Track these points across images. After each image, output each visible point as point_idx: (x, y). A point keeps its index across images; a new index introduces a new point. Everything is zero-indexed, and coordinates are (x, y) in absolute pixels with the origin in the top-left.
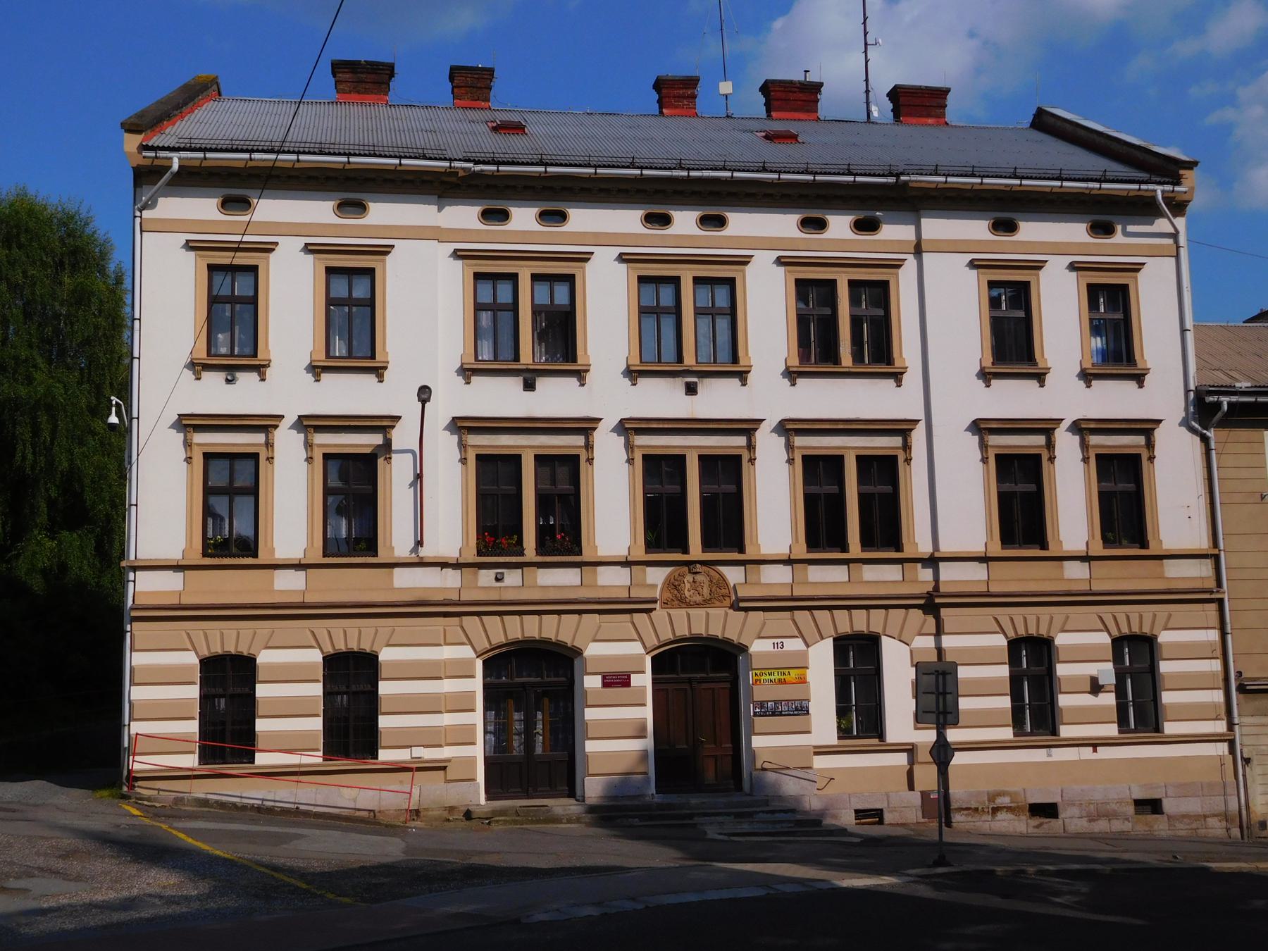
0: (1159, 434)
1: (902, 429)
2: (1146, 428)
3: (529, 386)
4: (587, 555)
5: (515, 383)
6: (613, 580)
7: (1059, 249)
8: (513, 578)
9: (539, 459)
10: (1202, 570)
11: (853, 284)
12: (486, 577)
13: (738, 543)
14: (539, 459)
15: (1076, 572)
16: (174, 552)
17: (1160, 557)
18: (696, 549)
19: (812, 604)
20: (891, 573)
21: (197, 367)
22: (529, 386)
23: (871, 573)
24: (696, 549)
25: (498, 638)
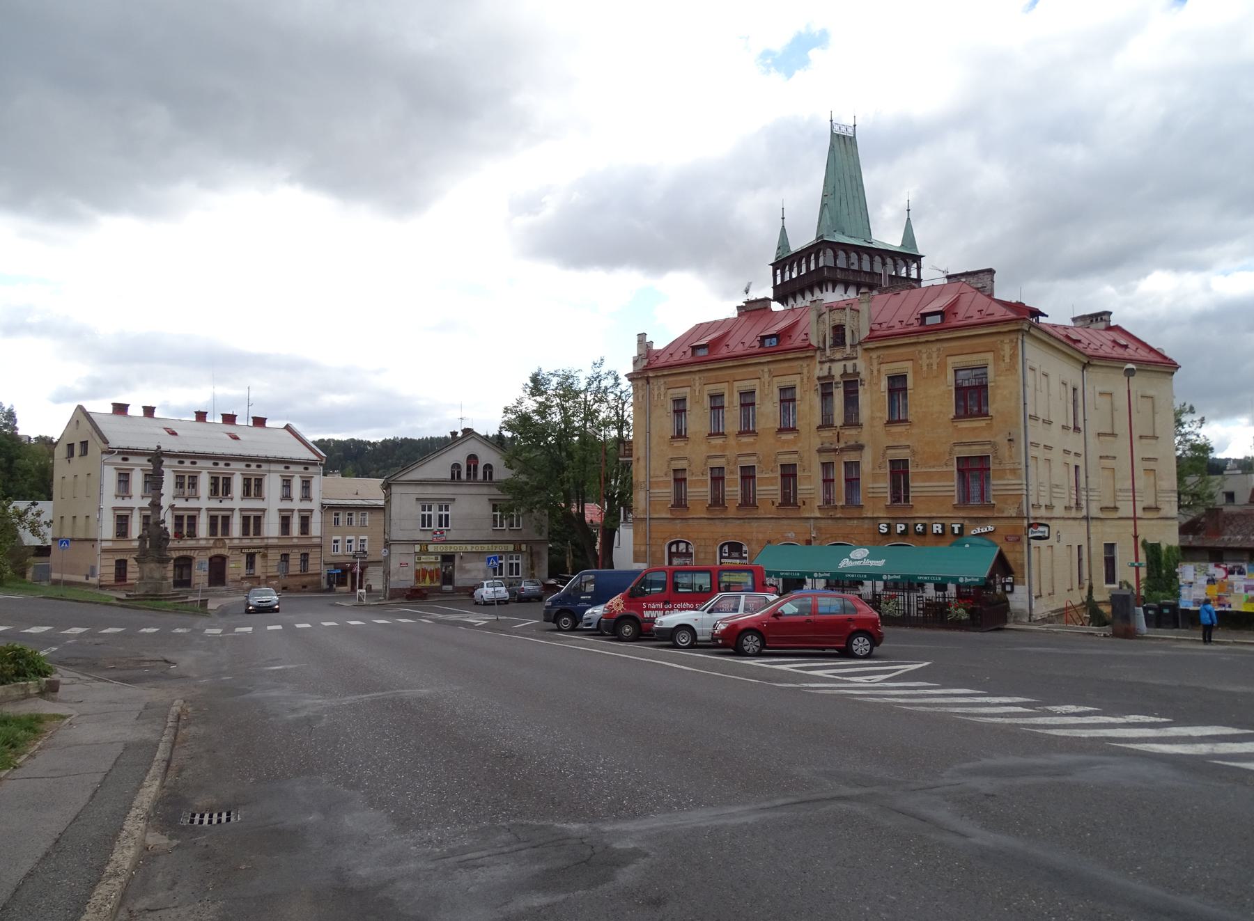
0: (314, 512)
1: (264, 510)
2: (311, 511)
3: (187, 500)
4: (197, 538)
5: (184, 500)
6: (203, 543)
7: (297, 473)
8: (181, 542)
9: (188, 517)
10: (319, 540)
11: (255, 479)
12: (176, 543)
13: (228, 535)
14: (188, 517)
15: (295, 541)
16: (110, 537)
17: (311, 538)
18: (219, 536)
19: (242, 548)
20: (258, 541)
21: (117, 496)
22: (187, 500)
23: (255, 541)
24: (219, 536)
25: (178, 555)
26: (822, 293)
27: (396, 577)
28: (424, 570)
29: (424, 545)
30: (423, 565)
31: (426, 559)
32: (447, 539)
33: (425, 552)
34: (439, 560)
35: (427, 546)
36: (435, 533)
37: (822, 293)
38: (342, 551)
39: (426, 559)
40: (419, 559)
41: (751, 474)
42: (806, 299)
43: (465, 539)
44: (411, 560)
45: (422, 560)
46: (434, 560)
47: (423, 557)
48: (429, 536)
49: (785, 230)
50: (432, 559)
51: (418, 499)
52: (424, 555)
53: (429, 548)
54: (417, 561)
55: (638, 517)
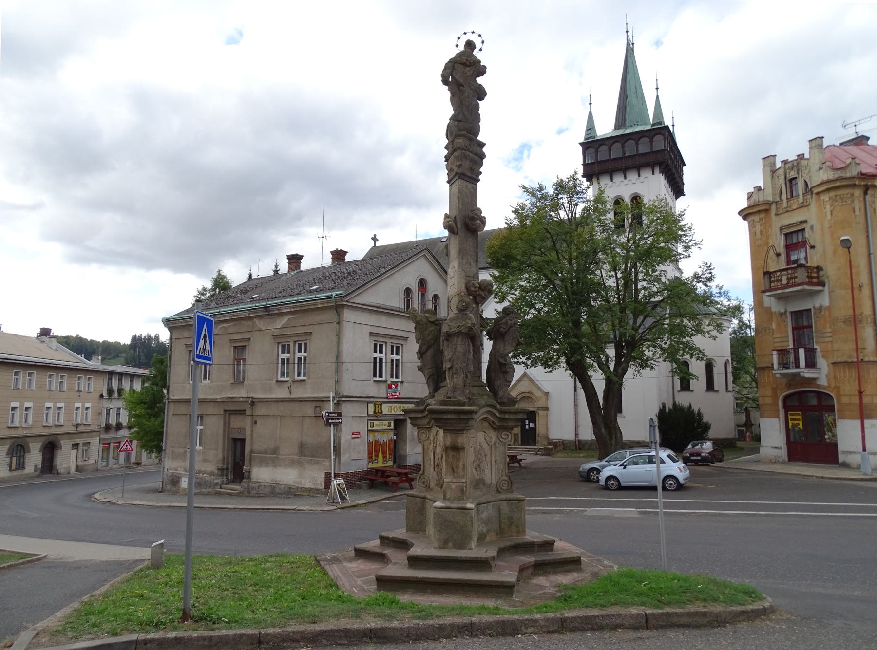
26: (653, 174)
27: (347, 455)
28: (377, 442)
29: (378, 403)
30: (376, 434)
31: (379, 425)
32: (402, 396)
33: (378, 415)
34: (392, 428)
35: (381, 405)
36: (390, 387)
37: (653, 174)
38: (53, 421)
39: (379, 425)
40: (372, 426)
41: (805, 323)
42: (628, 178)
43: (416, 397)
44: (362, 427)
45: (376, 428)
46: (387, 428)
47: (376, 422)
48: (380, 392)
49: (592, 115)
50: (385, 425)
51: (372, 334)
52: (378, 420)
53: (383, 410)
54: (370, 428)
55: (866, 359)
